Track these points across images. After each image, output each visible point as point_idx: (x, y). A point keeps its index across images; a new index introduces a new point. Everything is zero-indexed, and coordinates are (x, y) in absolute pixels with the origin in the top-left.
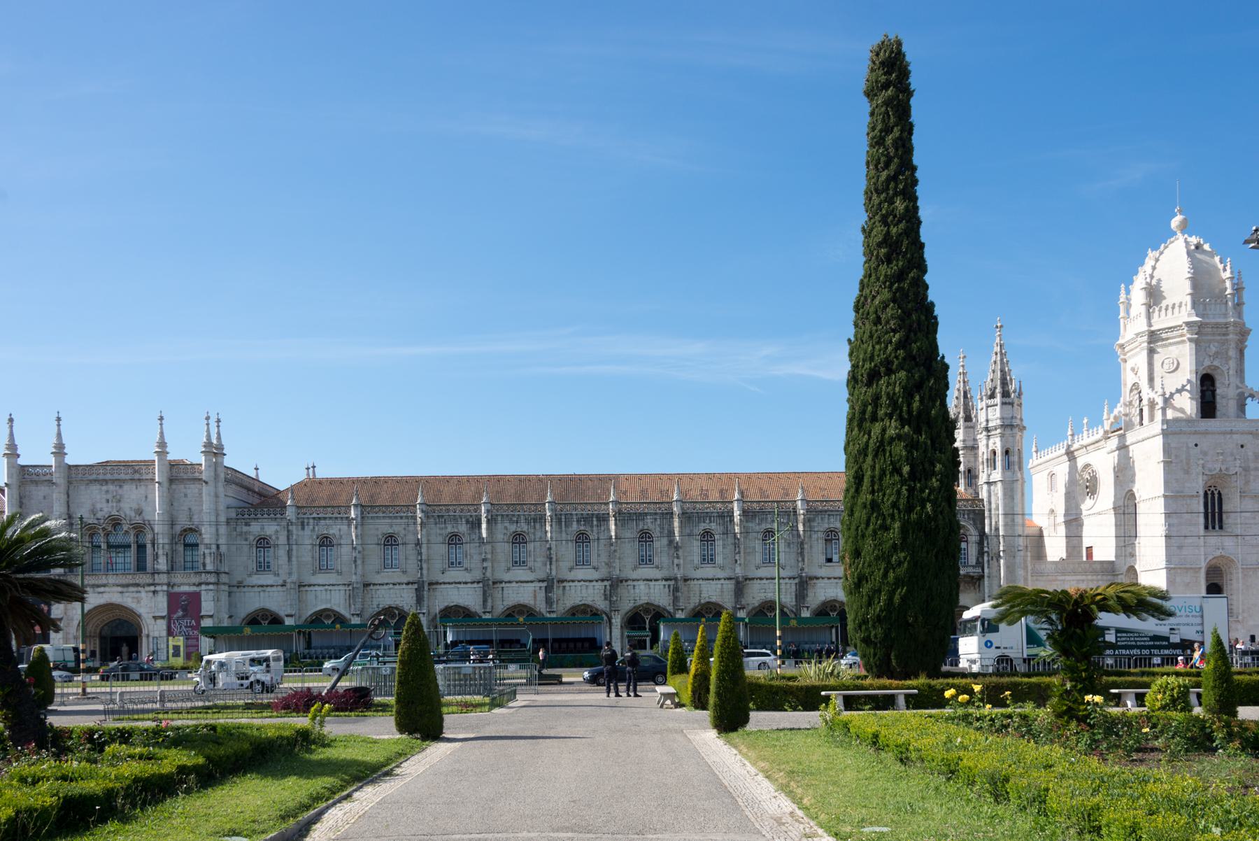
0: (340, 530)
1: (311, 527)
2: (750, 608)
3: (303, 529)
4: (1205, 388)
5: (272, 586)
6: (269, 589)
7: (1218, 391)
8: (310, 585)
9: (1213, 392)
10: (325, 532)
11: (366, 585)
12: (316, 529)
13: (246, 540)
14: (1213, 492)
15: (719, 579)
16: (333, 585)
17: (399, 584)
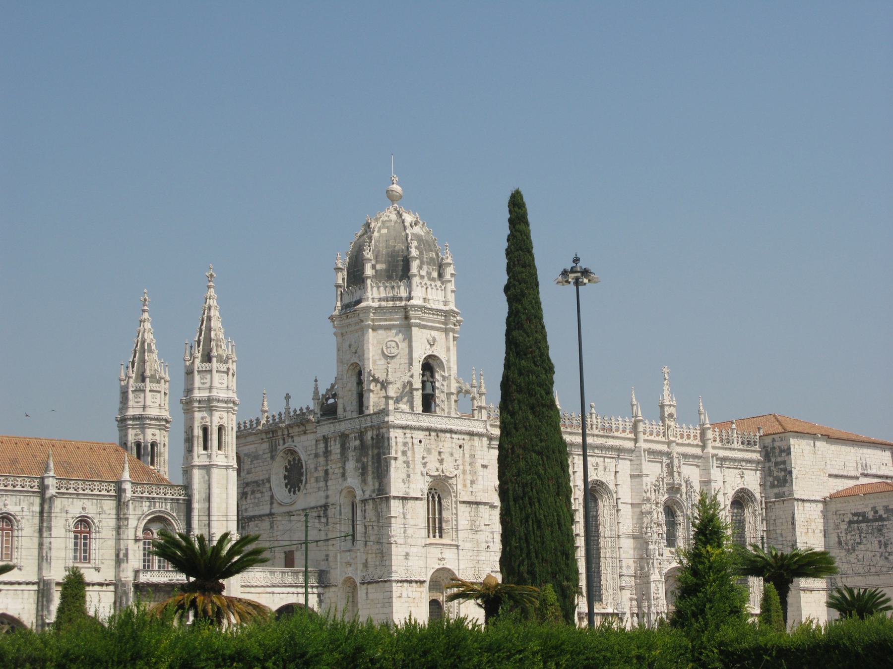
4: (425, 378)
7: (437, 384)
9: (433, 383)
14: (433, 495)
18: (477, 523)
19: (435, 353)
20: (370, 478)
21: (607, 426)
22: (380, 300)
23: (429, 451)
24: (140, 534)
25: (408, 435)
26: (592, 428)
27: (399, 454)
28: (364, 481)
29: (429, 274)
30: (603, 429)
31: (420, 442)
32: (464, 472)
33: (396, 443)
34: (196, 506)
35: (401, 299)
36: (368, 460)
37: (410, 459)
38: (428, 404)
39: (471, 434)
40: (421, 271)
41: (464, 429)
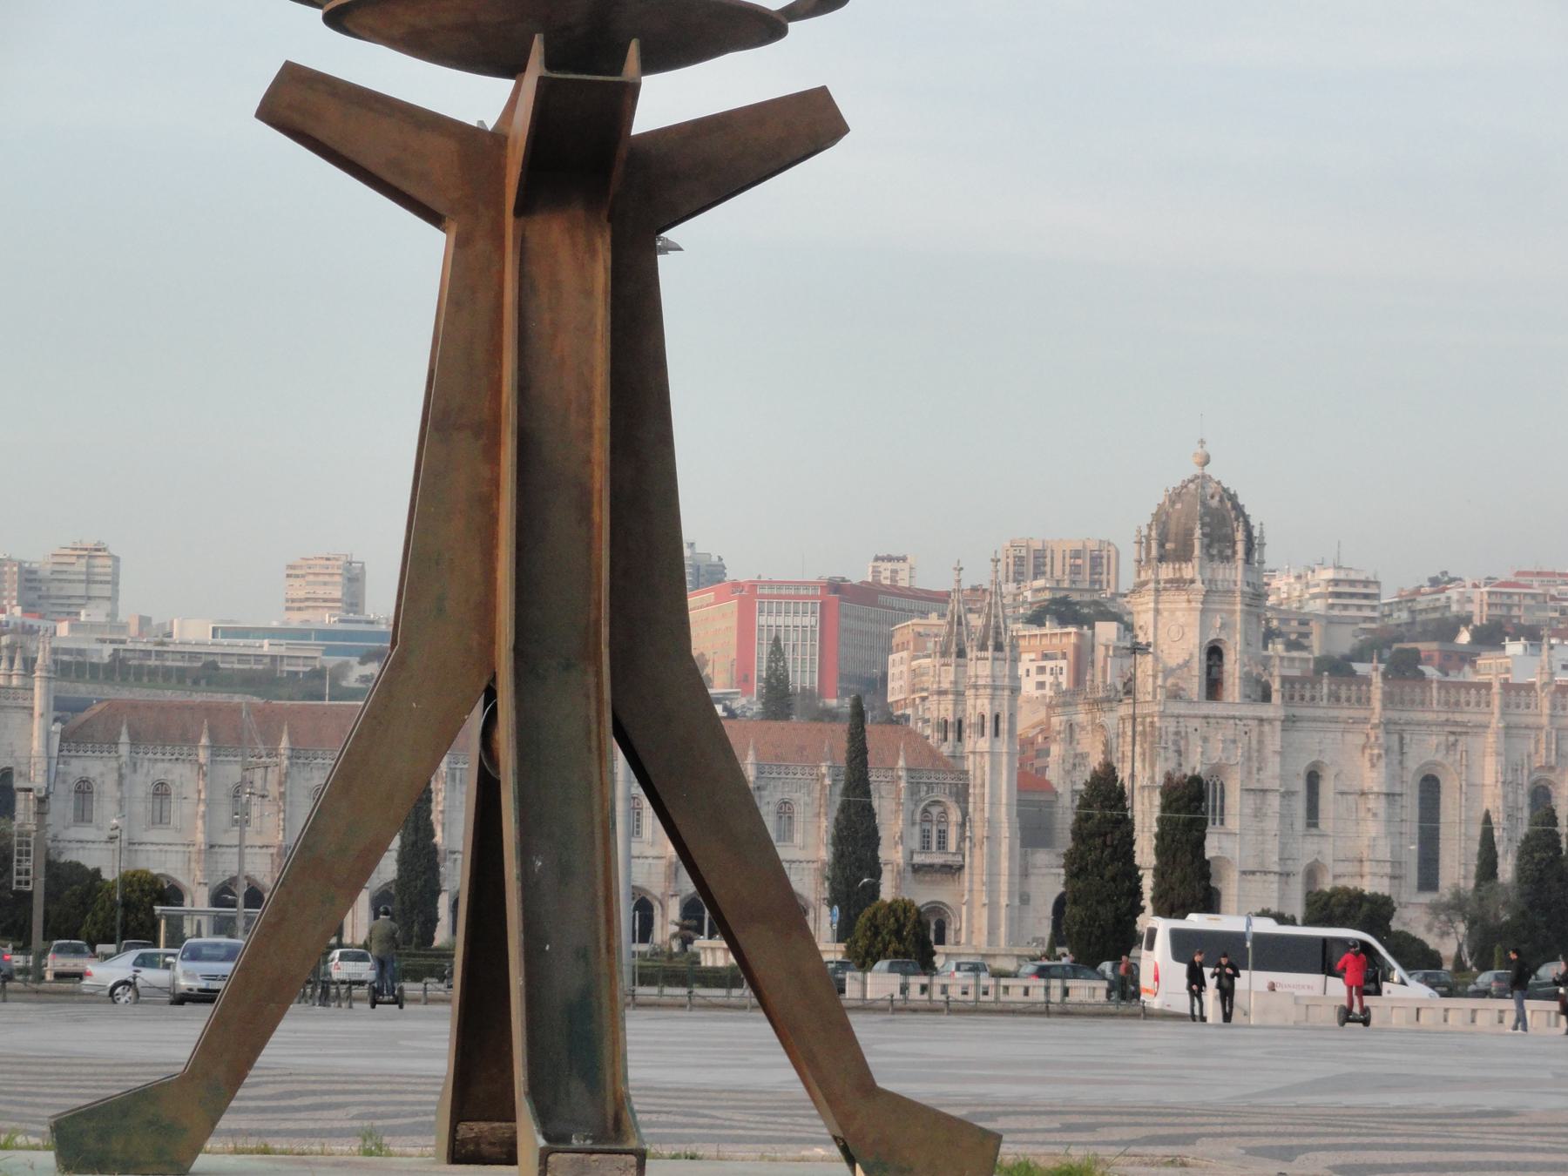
0: (181, 776)
1: (145, 770)
2: (683, 895)
3: (135, 771)
4: (1211, 663)
5: (93, 842)
6: (89, 845)
8: (140, 844)
10: (162, 777)
11: (212, 846)
12: (152, 772)
13: (64, 782)
15: (646, 857)
16: (170, 844)
17: (252, 847)
18: (1264, 810)
19: (1221, 637)
20: (1147, 766)
21: (1452, 700)
22: (1167, 582)
23: (1205, 740)
24: (918, 817)
25: (1181, 724)
26: (1431, 704)
27: (1170, 743)
28: (1144, 768)
29: (1221, 552)
30: (1447, 703)
31: (1196, 730)
32: (1249, 759)
33: (1167, 732)
34: (971, 791)
35: (1185, 582)
36: (1146, 746)
37: (1183, 748)
38: (1213, 687)
39: (1261, 720)
40: (1211, 550)
41: (1250, 714)
